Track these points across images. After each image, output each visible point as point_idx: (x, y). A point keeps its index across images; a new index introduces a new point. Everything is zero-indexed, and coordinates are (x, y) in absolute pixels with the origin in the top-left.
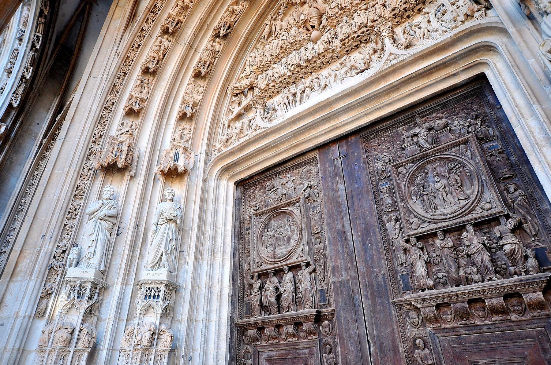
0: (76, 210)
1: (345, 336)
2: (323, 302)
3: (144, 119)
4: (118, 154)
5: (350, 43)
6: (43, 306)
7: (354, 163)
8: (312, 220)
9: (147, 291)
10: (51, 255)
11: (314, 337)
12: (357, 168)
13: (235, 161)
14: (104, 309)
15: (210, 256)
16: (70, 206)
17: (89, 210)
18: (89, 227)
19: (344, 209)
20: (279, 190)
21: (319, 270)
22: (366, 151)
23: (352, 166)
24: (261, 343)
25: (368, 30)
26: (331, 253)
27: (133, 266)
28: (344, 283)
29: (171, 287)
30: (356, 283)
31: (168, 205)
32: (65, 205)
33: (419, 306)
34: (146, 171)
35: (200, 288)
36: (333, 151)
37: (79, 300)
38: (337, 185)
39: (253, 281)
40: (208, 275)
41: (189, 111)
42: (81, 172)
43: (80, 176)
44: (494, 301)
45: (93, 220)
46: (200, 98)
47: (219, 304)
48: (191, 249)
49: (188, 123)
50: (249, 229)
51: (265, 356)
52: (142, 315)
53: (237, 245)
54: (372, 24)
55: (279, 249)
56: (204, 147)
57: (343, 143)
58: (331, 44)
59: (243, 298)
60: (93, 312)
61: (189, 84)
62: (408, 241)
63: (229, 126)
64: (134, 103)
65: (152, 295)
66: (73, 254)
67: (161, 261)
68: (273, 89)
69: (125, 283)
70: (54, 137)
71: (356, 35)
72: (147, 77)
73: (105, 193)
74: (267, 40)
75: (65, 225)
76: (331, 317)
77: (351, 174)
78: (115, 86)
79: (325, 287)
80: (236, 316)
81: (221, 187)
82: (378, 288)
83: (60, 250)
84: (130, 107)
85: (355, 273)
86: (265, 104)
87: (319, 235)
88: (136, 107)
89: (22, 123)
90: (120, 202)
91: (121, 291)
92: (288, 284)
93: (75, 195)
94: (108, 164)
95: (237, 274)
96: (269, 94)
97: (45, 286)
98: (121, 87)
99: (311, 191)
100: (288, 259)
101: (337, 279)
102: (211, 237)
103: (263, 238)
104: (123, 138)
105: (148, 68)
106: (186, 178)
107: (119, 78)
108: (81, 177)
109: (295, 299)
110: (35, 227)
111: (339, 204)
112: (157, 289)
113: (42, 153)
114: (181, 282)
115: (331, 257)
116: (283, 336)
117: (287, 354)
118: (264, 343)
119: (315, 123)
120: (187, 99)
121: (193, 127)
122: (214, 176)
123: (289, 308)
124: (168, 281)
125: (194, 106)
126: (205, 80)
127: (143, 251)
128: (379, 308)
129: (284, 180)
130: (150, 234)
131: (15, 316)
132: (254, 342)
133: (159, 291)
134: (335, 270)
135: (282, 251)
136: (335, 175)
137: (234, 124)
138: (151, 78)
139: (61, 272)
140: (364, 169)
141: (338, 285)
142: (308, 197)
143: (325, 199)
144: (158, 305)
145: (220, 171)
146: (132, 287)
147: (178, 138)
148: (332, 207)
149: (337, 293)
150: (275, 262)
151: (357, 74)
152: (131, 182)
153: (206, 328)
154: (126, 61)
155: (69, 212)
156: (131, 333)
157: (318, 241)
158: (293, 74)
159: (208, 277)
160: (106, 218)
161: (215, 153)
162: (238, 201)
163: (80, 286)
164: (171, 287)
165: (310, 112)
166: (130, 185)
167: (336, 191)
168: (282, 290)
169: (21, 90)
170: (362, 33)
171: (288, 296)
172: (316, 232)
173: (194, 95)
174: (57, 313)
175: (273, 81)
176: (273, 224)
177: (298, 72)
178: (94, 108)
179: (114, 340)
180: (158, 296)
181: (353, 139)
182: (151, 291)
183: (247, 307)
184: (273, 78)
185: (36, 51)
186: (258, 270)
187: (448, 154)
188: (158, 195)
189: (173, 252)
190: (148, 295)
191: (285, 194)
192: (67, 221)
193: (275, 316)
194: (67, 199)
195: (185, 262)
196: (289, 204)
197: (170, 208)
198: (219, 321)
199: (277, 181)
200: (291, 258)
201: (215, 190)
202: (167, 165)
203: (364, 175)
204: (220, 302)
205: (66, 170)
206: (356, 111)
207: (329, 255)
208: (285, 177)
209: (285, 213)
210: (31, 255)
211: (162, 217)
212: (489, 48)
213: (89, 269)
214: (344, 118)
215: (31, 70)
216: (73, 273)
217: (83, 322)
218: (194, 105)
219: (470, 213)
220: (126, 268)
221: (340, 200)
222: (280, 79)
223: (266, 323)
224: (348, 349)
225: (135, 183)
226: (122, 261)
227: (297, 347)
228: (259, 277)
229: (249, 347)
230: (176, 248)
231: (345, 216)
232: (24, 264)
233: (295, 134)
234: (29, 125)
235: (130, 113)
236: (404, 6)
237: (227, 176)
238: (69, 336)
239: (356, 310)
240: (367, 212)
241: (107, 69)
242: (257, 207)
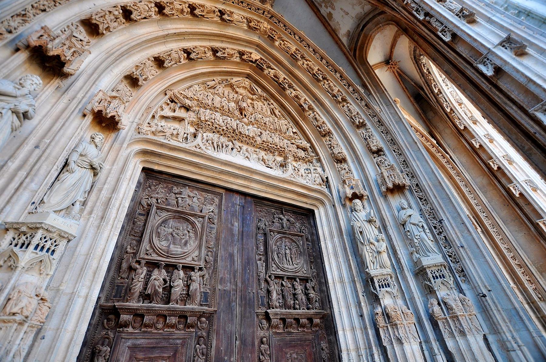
1: (221, 331)
12: (248, 218)
30: (234, 294)
33: (272, 317)
36: (236, 198)
39: (138, 266)
44: (304, 320)
51: (129, 343)
53: (126, 225)
57: (243, 197)
62: (270, 277)
82: (249, 301)
84: (98, 23)
87: (210, 250)
111: (233, 235)
117: (157, 343)
128: (248, 314)
129: (192, 195)
133: (56, 246)
136: (234, 215)
141: (223, 292)
167: (233, 225)
175: (212, 123)
176: (171, 222)
180: (54, 251)
181: (249, 199)
183: (117, 289)
184: (213, 121)
186: (146, 257)
187: (294, 238)
199: (186, 191)
200: (185, 259)
209: (188, 220)
212: (322, 203)
214: (254, 185)
219: (298, 272)
222: (217, 126)
227: (170, 337)
229: (109, 333)
231: (235, 245)
233: (222, 172)
239: (232, 314)
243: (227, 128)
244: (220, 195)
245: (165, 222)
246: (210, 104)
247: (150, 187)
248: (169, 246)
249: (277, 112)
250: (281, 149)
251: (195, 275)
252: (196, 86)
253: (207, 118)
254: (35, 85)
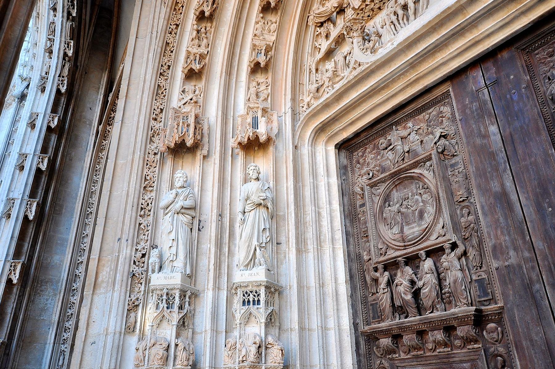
0: (148, 204)
1: (524, 343)
2: (484, 297)
3: (208, 81)
4: (185, 130)
6: (132, 320)
7: (510, 91)
8: (453, 183)
9: (244, 295)
10: (130, 261)
11: (476, 346)
12: (515, 97)
13: (332, 117)
14: (198, 320)
15: (315, 246)
16: (141, 201)
17: (163, 203)
18: (166, 223)
19: (502, 161)
20: (399, 147)
21: (472, 253)
22: (530, 69)
23: (508, 96)
24: (400, 356)
26: (487, 227)
27: (223, 266)
28: (514, 268)
29: (272, 290)
31: (253, 186)
32: (136, 200)
34: (221, 146)
35: (308, 288)
36: (474, 78)
37: (169, 311)
38: (486, 127)
39: (378, 274)
40: (317, 271)
41: (262, 60)
42: (147, 158)
43: (146, 163)
45: (169, 214)
46: (274, 38)
47: (335, 307)
48: (290, 240)
49: (263, 75)
50: (363, 205)
52: (242, 325)
55: (410, 229)
56: (289, 104)
57: (489, 64)
59: (366, 297)
60: (186, 324)
61: (257, 23)
63: (317, 70)
64: (193, 62)
65: (251, 300)
66: (153, 258)
67: (255, 258)
68: (372, 6)
69: (217, 288)
70: (110, 122)
72: (203, 25)
73: (177, 180)
75: (140, 224)
76: (499, 317)
77: (507, 108)
78: (167, 44)
79: (484, 276)
80: (360, 321)
81: (317, 154)
83: (139, 255)
84: (189, 68)
85: (529, 251)
86: (363, 29)
87: (466, 203)
88: (196, 67)
89: (73, 110)
90: (196, 190)
91: (214, 297)
92: (428, 275)
93: (145, 187)
94: (176, 144)
95: (355, 266)
96: (367, 14)
97: (130, 297)
98: (175, 45)
99: (447, 143)
100: (424, 241)
101: (501, 263)
102: (314, 220)
103: (384, 215)
104: (187, 108)
105: (203, 12)
106: (271, 149)
107: (171, 33)
108: (147, 164)
109: (440, 295)
110: (108, 229)
111: (492, 155)
112: (256, 292)
113: (101, 142)
114: (283, 282)
115: (489, 233)
116: (430, 346)
118: (403, 356)
119: (442, 42)
120: (257, 44)
121: (270, 79)
122: (307, 141)
123: (433, 308)
124: (267, 282)
125: (268, 52)
126: (277, 13)
127: (232, 248)
129: (404, 133)
130: (237, 225)
131: (105, 333)
132: (390, 354)
133: (258, 295)
134: (498, 251)
135: (413, 230)
136: (482, 113)
137: (324, 66)
138: (209, 25)
139: (144, 279)
140: (528, 98)
141: (505, 272)
142: (443, 151)
143: (469, 151)
144: (261, 313)
145: (314, 132)
146: (225, 293)
147: (254, 97)
148: (481, 162)
149: (503, 283)
150: (405, 246)
152: (205, 163)
153: (323, 339)
154: (175, 9)
155: (142, 209)
156: (234, 347)
157: (465, 211)
159: (317, 274)
160: (183, 211)
161: (304, 109)
162: (343, 170)
163: (167, 294)
164: (272, 290)
165: (432, 27)
166: (205, 167)
167: (486, 136)
168: (420, 284)
169: (66, 72)
171: (430, 291)
172: (461, 200)
173: (266, 36)
174: (147, 327)
176: (396, 195)
178: (148, 77)
179: (214, 356)
180: (259, 301)
181: (505, 54)
182: (249, 295)
185: (73, 19)
186: (382, 258)
188: (239, 175)
189: (268, 244)
190: (246, 300)
191: (408, 152)
192: (141, 219)
193: (413, 319)
194: (137, 192)
195: (285, 257)
196: (415, 165)
197: (257, 190)
198: (339, 329)
199: (394, 136)
200: (427, 239)
201: (310, 159)
202: (244, 135)
203: (529, 107)
204: (337, 304)
205: (130, 158)
206: (506, 10)
207: (485, 230)
208: (405, 128)
209: (412, 178)
210: (110, 263)
211: (248, 202)
213: (174, 274)
215: (72, 44)
216: (158, 280)
217: (178, 336)
218: (268, 49)
220: (215, 270)
221: (494, 148)
223: (403, 329)
224: (532, 361)
225: (210, 163)
226: (209, 262)
227: (451, 360)
228: (386, 268)
229: (383, 361)
230: (271, 240)
231: (505, 171)
232: (104, 273)
233: (413, 65)
234: (82, 112)
235: (192, 75)
237: (324, 138)
238: (165, 352)
239: (538, 306)
240: (539, 160)
241: (156, 24)
242: (371, 175)
244: (446, 95)
245: (387, 199)
247: (359, 163)
248: (402, 231)
251: (449, 260)
254: (181, 179)
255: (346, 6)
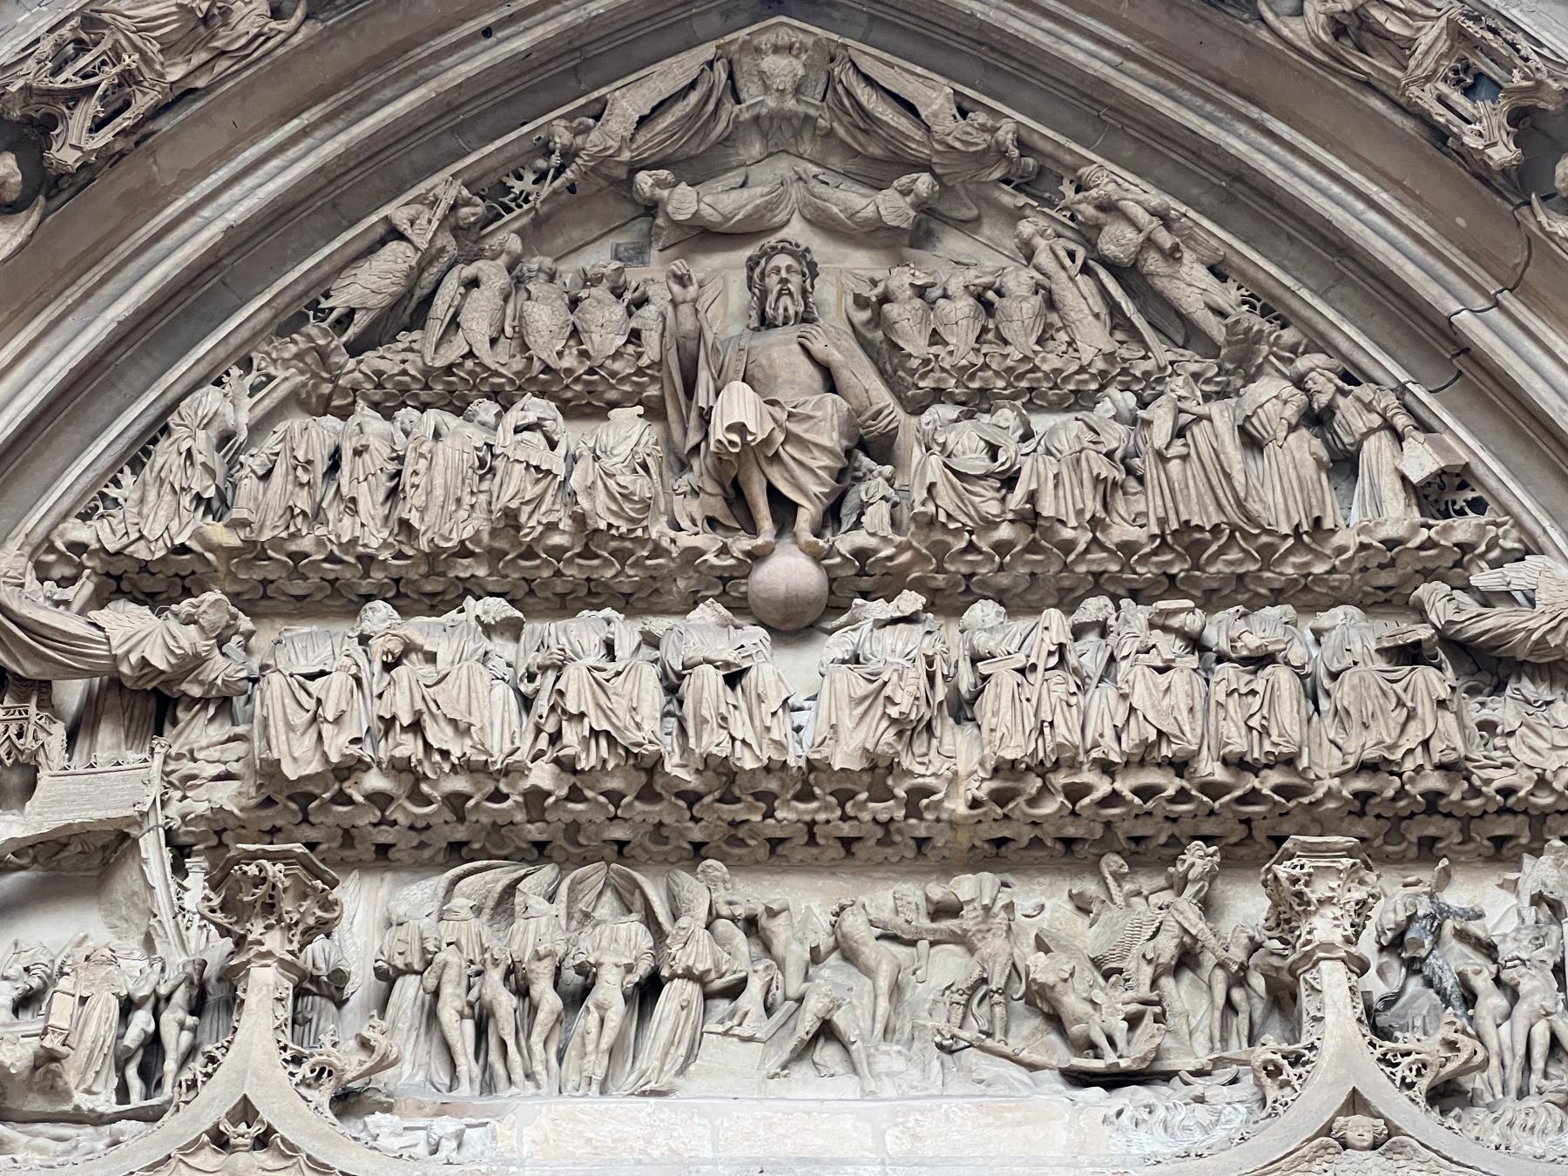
5: (1049, 808)
25: (1182, 796)
54: (1220, 774)
58: (920, 747)
71: (1103, 787)
74: (354, 349)
151: (1078, 1079)
158: (575, 795)
170: (1145, 792)
175: (400, 768)
177: (615, 797)
184: (409, 747)
222: (460, 784)
236: (1434, 781)
243: (566, 765)
246: (375, 538)
249: (1192, 287)
250: (1253, 782)
252: (210, 399)
253: (337, 746)
255: (196, 691)
